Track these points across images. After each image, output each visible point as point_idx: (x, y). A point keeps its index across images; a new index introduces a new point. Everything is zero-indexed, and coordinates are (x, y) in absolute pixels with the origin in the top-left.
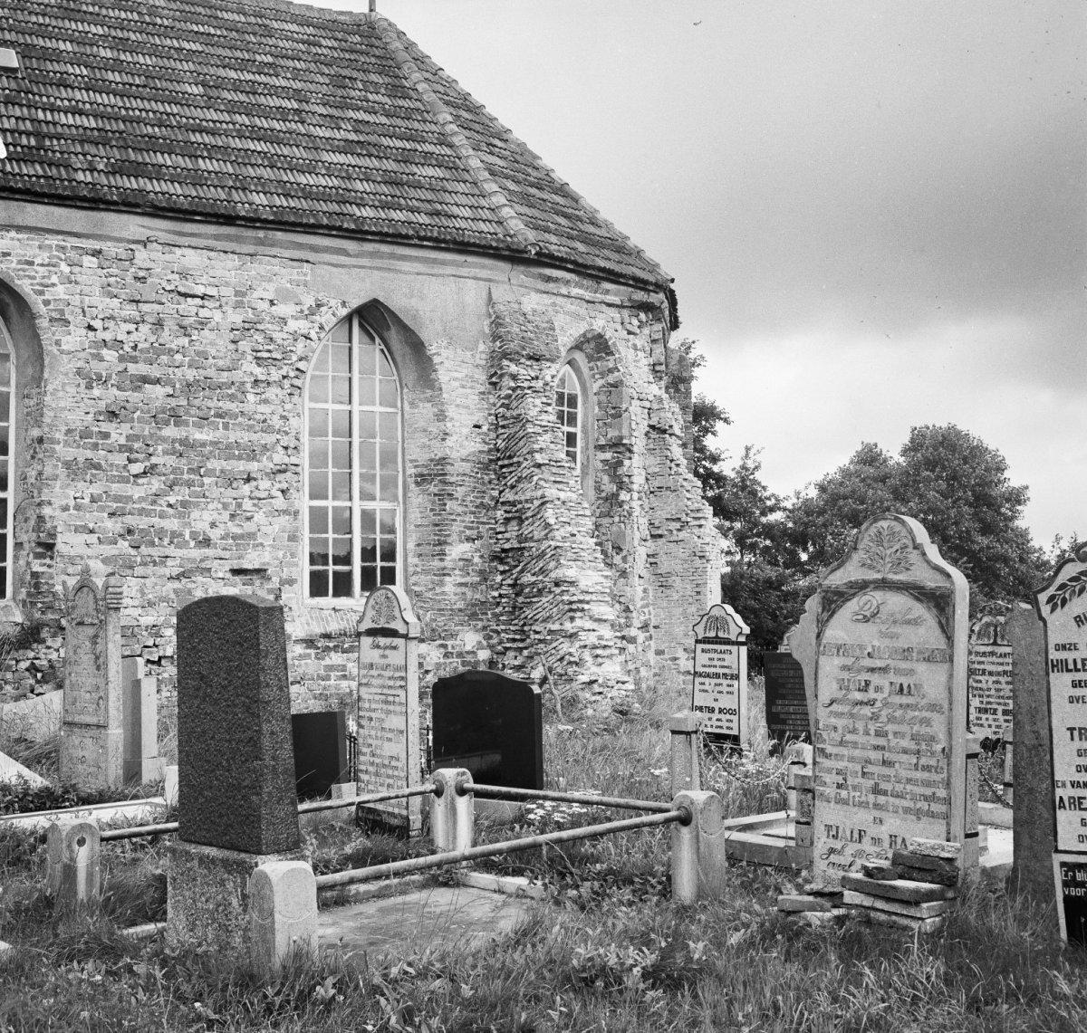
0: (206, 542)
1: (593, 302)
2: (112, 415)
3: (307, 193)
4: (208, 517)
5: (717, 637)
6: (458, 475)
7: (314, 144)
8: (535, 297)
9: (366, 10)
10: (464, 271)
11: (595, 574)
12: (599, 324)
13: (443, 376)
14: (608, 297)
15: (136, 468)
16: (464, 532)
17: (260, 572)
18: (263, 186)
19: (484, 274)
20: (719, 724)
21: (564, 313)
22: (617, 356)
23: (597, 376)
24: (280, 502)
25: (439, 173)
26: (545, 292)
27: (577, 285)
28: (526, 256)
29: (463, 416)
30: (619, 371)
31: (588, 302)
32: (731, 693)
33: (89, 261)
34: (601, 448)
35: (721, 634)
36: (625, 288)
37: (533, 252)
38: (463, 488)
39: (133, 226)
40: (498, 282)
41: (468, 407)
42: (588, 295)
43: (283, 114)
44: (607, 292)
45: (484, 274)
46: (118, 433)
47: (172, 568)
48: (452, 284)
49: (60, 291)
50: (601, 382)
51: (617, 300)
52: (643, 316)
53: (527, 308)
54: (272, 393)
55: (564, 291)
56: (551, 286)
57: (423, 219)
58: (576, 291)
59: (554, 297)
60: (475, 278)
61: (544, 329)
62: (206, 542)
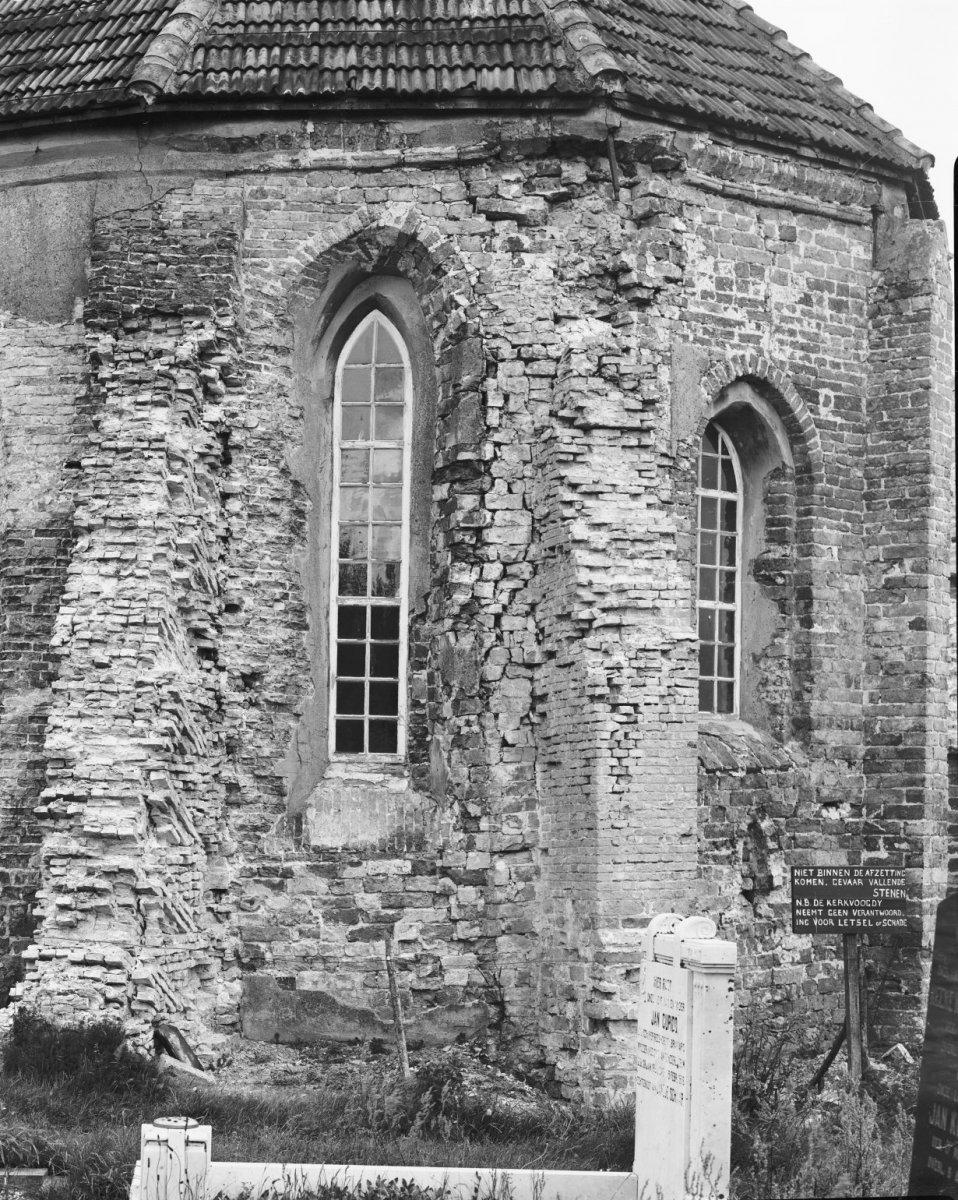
1: (379, 170)
6: (30, 561)
8: (204, 187)
10: (41, 171)
11: (125, 741)
12: (394, 215)
14: (420, 150)
16: (45, 667)
19: (84, 165)
21: (290, 207)
22: (451, 273)
26: (229, 174)
27: (316, 141)
28: (138, 110)
29: (42, 449)
30: (458, 306)
34: (437, 477)
36: (469, 121)
37: (150, 101)
38: (41, 584)
40: (114, 175)
41: (51, 431)
44: (415, 140)
45: (84, 165)
48: (21, 199)
50: (442, 336)
51: (449, 151)
56: (247, 159)
58: (310, 156)
59: (259, 179)
60: (63, 179)
61: (202, 250)
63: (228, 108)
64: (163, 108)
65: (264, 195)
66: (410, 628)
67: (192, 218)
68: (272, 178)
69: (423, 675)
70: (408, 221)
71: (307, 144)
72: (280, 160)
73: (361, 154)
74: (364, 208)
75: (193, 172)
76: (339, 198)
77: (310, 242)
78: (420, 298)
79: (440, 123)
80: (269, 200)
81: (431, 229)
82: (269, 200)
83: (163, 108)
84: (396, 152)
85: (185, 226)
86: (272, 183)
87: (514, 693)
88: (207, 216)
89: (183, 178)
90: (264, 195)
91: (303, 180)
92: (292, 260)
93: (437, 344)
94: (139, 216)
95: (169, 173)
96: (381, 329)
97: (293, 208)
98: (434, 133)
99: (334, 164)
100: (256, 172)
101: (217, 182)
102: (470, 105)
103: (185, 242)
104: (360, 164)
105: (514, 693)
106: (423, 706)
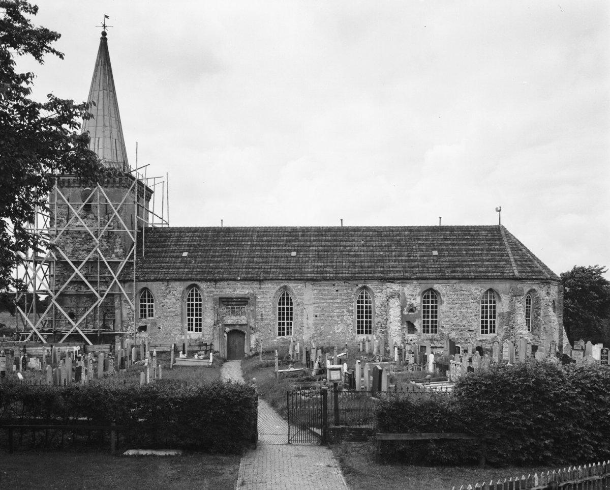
0: (465, 326)
2: (451, 308)
3: (481, 272)
4: (465, 322)
7: (483, 261)
9: (498, 224)
12: (534, 287)
13: (502, 299)
15: (455, 316)
17: (473, 331)
18: (473, 272)
24: (476, 320)
25: (505, 263)
33: (448, 287)
34: (535, 309)
39: (454, 281)
43: (478, 255)
46: (452, 311)
47: (460, 330)
49: (444, 292)
53: (518, 287)
54: (474, 304)
57: (499, 274)
58: (528, 282)
62: (465, 326)
87: (543, 327)
105: (543, 327)
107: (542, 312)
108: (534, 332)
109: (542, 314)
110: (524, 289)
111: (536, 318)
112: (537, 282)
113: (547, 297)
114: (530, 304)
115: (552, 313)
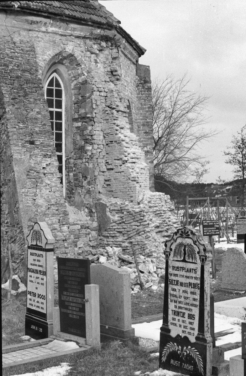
1: (65, 36)
5: (37, 245)
8: (24, 33)
12: (69, 48)
14: (75, 32)
20: (38, 304)
22: (83, 66)
23: (73, 79)
26: (30, 30)
27: (52, 25)
28: (13, 9)
30: (84, 75)
31: (62, 35)
32: (42, 284)
34: (75, 120)
35: (39, 244)
36: (87, 27)
37: (16, 6)
42: (61, 31)
44: (74, 29)
50: (75, 82)
51: (82, 34)
52: (104, 44)
53: (17, 39)
55: (43, 29)
58: (51, 29)
61: (27, 51)
63: (35, 12)
64: (19, 9)
65: (38, 38)
66: (66, 161)
67: (22, 41)
68: (40, 33)
69: (71, 174)
70: (73, 51)
71: (50, 26)
72: (43, 29)
73: (62, 31)
74: (62, 45)
75: (20, 28)
76: (56, 42)
77: (50, 53)
78: (68, 71)
79: (81, 26)
80: (40, 39)
81: (78, 54)
82: (40, 39)
83: (19, 9)
84: (70, 32)
85: (20, 43)
86: (40, 35)
87: (101, 179)
88: (26, 41)
89: (17, 29)
90: (38, 38)
91: (48, 35)
92: (46, 57)
93: (73, 85)
94: (6, 38)
95: (13, 27)
96: (56, 78)
97: (45, 42)
98: (79, 28)
99: (57, 32)
100: (37, 31)
101: (26, 32)
102: (90, 23)
103: (22, 48)
104: (62, 33)
105: (101, 179)
106: (72, 183)
107: (97, 131)
108: (77, 198)
109: (99, 137)
110: (38, 50)
111: (82, 149)
112: (77, 33)
113: (112, 86)
114: (59, 105)
115: (127, 132)
